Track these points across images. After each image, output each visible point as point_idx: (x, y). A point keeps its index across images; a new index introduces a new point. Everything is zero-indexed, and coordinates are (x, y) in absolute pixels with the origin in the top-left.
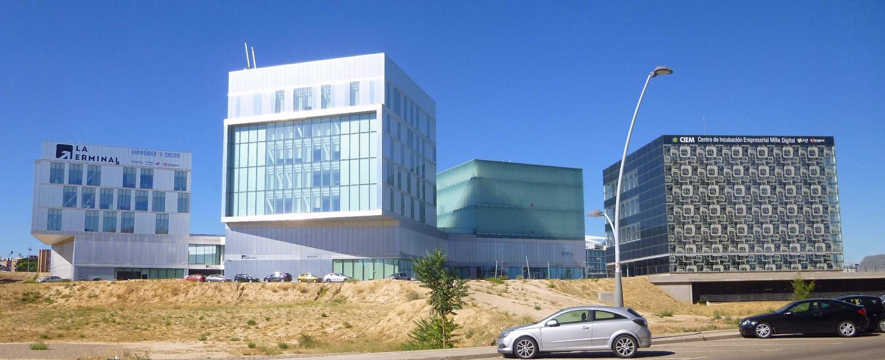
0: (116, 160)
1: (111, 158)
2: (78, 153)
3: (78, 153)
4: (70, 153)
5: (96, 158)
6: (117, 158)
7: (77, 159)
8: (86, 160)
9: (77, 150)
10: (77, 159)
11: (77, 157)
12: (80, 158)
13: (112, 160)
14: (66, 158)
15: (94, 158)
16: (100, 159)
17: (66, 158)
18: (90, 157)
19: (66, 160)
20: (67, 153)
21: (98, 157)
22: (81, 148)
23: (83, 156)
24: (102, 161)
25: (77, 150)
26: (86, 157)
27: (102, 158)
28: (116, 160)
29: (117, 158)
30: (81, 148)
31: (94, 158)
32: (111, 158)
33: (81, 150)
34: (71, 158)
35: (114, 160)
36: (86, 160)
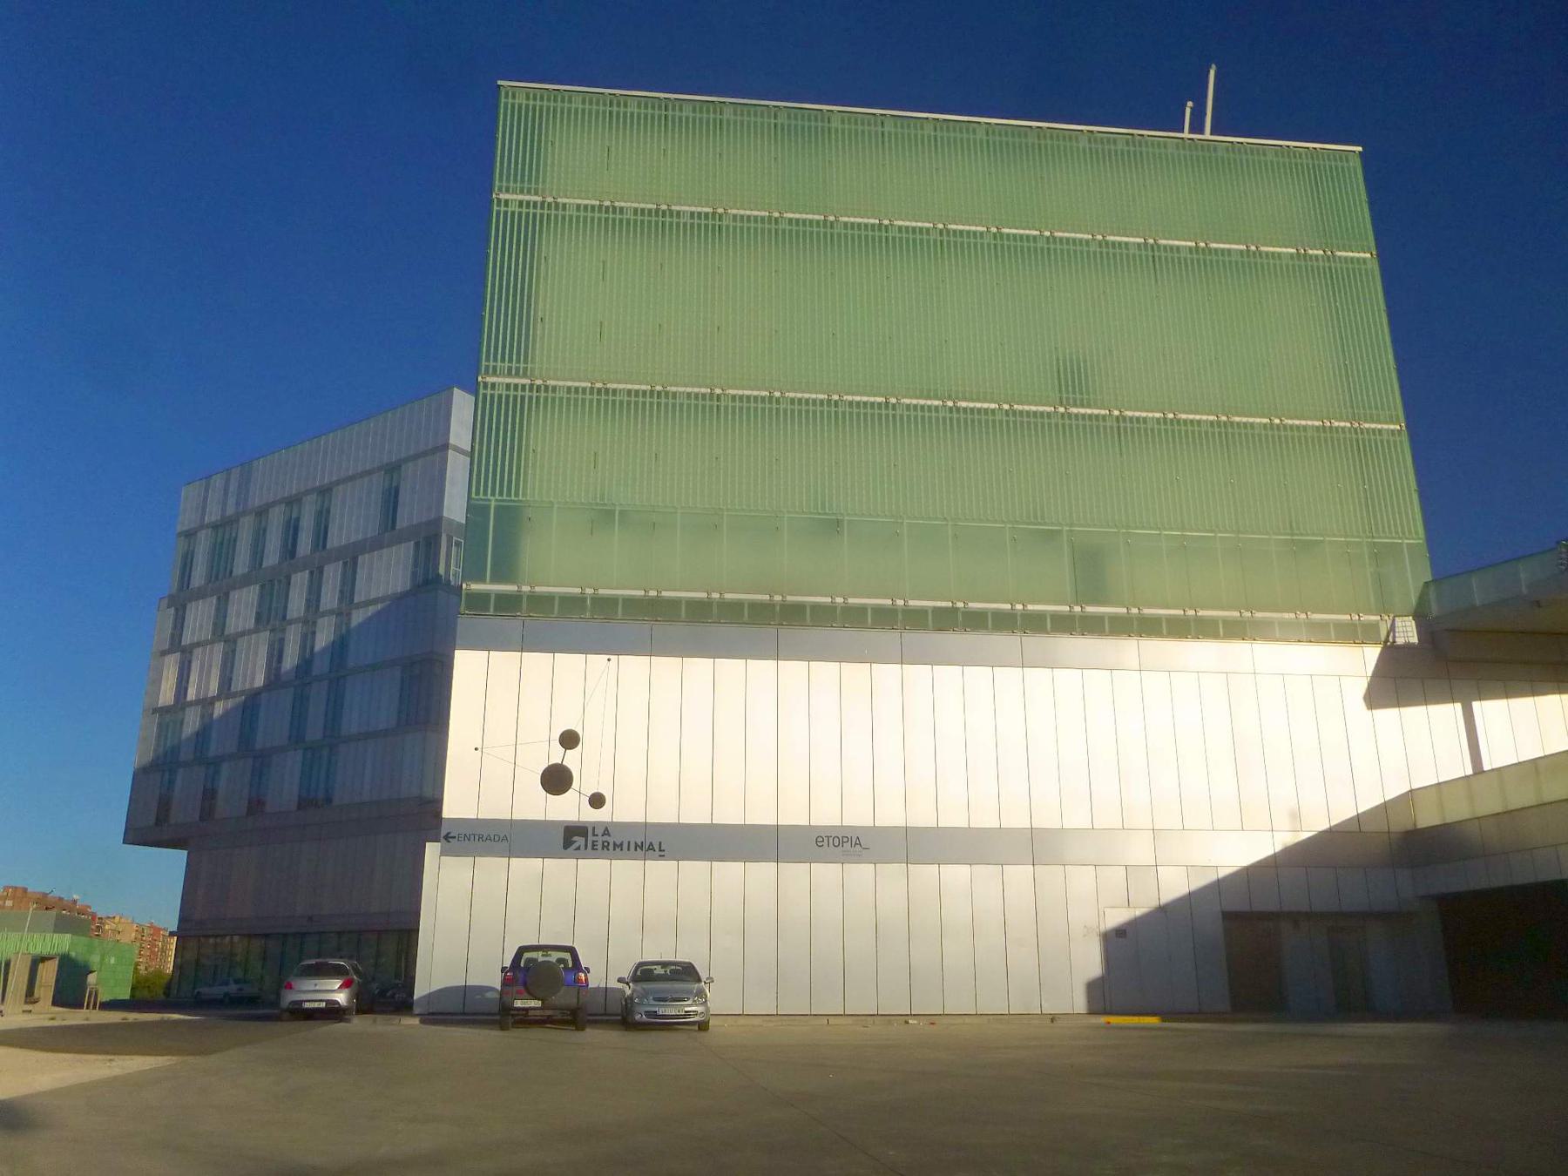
0: (660, 847)
1: (651, 844)
2: (595, 838)
3: (595, 838)
4: (584, 839)
5: (625, 846)
6: (660, 843)
7: (593, 849)
8: (608, 850)
9: (594, 835)
10: (593, 849)
11: (593, 845)
12: (600, 847)
13: (651, 847)
14: (578, 848)
15: (621, 844)
16: (625, 846)
17: (578, 848)
18: (615, 844)
19: (578, 851)
20: (580, 841)
21: (629, 842)
22: (599, 831)
23: (603, 843)
24: (636, 850)
25: (594, 835)
26: (608, 843)
27: (636, 845)
28: (660, 847)
29: (660, 843)
30: (599, 831)
31: (621, 844)
32: (651, 844)
33: (600, 835)
34: (586, 848)
35: (657, 847)
36: (608, 850)
